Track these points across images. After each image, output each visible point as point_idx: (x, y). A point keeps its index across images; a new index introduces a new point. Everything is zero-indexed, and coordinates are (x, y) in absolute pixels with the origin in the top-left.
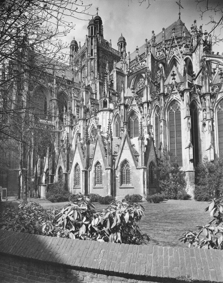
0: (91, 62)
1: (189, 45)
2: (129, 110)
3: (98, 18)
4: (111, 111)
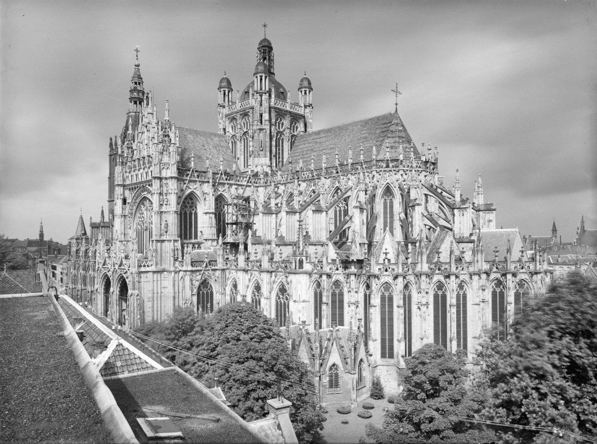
0: (259, 135)
1: (407, 170)
2: (332, 281)
3: (266, 44)
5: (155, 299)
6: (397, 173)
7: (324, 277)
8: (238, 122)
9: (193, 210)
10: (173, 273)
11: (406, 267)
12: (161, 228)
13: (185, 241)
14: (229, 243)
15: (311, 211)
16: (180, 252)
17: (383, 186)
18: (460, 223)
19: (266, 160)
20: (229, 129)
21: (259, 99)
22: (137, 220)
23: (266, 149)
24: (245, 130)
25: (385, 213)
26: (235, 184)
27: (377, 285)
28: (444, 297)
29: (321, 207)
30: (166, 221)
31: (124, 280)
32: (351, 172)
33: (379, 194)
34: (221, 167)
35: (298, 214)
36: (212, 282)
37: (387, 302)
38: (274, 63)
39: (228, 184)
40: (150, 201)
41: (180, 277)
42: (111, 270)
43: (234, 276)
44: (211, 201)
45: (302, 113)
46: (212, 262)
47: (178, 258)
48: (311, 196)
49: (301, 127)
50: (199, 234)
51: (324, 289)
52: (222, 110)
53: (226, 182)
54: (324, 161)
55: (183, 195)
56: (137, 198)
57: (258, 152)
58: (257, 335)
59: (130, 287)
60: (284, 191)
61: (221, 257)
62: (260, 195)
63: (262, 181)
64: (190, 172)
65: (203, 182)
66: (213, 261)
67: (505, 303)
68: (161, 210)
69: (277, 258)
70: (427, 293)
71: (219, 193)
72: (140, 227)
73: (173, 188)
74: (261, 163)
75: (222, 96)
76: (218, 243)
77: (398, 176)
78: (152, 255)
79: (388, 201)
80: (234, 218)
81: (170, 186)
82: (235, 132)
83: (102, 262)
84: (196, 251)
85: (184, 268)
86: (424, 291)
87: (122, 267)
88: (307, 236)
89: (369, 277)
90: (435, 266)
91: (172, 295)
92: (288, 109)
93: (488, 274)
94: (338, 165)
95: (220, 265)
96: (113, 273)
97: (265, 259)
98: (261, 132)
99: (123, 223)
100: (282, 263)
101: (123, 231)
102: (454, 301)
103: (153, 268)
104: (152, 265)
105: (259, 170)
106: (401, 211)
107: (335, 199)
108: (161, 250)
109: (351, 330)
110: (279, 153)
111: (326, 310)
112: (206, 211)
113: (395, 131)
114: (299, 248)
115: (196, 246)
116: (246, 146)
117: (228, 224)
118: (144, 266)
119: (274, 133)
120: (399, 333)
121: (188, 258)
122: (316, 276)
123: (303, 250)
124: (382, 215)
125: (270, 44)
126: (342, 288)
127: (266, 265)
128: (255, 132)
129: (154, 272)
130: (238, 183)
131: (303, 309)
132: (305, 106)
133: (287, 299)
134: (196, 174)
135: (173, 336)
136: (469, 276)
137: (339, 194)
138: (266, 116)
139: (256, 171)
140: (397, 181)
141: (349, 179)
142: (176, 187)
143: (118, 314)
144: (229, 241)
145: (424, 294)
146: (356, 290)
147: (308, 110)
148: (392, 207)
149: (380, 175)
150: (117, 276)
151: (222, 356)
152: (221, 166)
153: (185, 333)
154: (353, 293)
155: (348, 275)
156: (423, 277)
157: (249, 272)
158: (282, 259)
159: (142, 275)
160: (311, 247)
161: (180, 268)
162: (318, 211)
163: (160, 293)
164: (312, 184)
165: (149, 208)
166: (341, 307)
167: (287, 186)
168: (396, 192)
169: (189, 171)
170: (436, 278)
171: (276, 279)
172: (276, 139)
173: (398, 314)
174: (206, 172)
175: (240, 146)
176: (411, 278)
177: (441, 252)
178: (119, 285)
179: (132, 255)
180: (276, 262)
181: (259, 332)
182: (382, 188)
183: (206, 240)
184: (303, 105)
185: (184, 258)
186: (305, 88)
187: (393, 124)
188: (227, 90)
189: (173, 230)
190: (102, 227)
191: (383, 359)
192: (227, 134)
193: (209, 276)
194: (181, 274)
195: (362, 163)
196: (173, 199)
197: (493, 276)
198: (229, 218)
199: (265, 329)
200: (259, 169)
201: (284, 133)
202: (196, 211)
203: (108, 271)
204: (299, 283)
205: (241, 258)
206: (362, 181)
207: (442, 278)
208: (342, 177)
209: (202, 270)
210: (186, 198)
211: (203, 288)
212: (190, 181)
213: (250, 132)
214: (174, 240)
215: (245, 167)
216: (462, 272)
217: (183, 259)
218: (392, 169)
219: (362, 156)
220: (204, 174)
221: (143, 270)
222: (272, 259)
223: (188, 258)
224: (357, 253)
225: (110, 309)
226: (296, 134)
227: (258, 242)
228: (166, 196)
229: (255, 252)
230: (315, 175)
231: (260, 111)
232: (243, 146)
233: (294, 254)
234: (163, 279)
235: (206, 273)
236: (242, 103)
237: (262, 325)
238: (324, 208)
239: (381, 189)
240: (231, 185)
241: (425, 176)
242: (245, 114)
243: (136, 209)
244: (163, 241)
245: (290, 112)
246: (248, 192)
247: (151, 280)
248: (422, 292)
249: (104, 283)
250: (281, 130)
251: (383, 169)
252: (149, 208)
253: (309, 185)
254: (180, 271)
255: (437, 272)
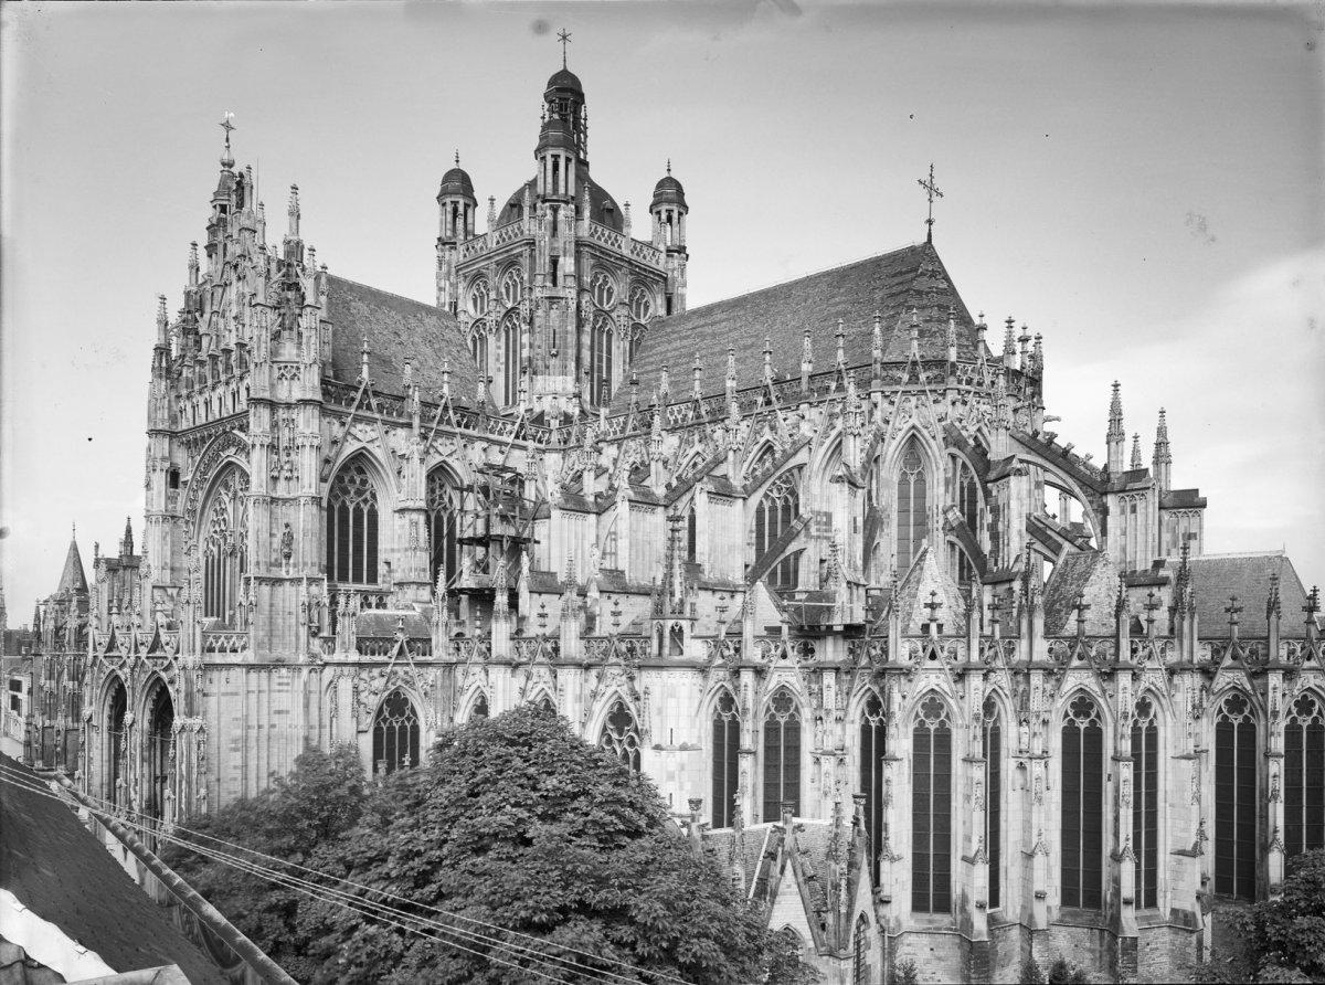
0: (547, 314)
1: (969, 392)
2: (771, 686)
4: (692, 666)
5: (252, 743)
6: (940, 398)
7: (747, 677)
8: (491, 284)
9: (365, 501)
10: (305, 671)
11: (990, 648)
12: (271, 543)
13: (342, 586)
14: (462, 591)
15: (705, 496)
16: (326, 612)
17: (901, 434)
18: (1124, 533)
19: (565, 382)
20: (466, 305)
21: (549, 217)
22: (207, 529)
23: (566, 353)
24: (509, 305)
25: (903, 511)
26: (480, 439)
27: (904, 697)
28: (1095, 735)
29: (730, 486)
30: (287, 526)
31: (164, 690)
32: (807, 398)
33: (888, 459)
34: (446, 389)
35: (660, 510)
36: (415, 698)
37: (933, 749)
38: (586, 137)
39: (463, 436)
40: (245, 475)
41: (326, 682)
42: (128, 661)
43: (478, 683)
44: (417, 474)
45: (660, 267)
46: (419, 643)
47: (319, 629)
48: (695, 465)
49: (658, 307)
50: (382, 569)
51: (745, 710)
52: (447, 253)
53: (458, 430)
54: (732, 372)
55: (338, 454)
56: (208, 466)
57: (544, 359)
58: (594, 822)
59: (179, 705)
60: (615, 461)
61: (441, 629)
62: (548, 474)
63: (555, 437)
64: (358, 396)
65: (396, 425)
66: (419, 640)
67: (1259, 756)
68: (274, 495)
69: (604, 627)
70: (1045, 723)
71: (439, 459)
72: (215, 550)
73: (307, 432)
74: (555, 391)
75: (450, 217)
76: (433, 593)
77: (944, 407)
78: (246, 621)
79: (912, 479)
80: (480, 523)
81: (301, 427)
82: (482, 309)
83: (106, 640)
84: (373, 611)
85: (338, 656)
86: (1038, 717)
87: (158, 654)
88: (692, 567)
89: (881, 674)
90: (1070, 647)
91: (301, 733)
92: (626, 252)
93: (1208, 672)
94: (770, 382)
95: (441, 649)
96: (133, 670)
97: (573, 628)
98: (555, 306)
99: (168, 538)
100: (621, 640)
101: (168, 561)
102: (1126, 746)
103: (250, 656)
104: (244, 648)
105: (547, 409)
106: (949, 503)
107: (768, 469)
108: (271, 605)
109: (837, 826)
110: (600, 368)
111: (751, 771)
112: (403, 505)
113: (927, 293)
114: (672, 594)
115: (373, 600)
116: (511, 349)
117: (461, 541)
118: (222, 650)
119: (588, 311)
120: (968, 839)
121: (347, 630)
122: (721, 674)
123: (682, 602)
124: (894, 516)
125: (580, 85)
126: (797, 709)
127: (572, 646)
128: (537, 306)
129: (250, 667)
130: (495, 437)
131: (683, 769)
132: (668, 251)
133: (632, 743)
134: (374, 402)
135: (291, 840)
136: (1166, 677)
137: (777, 456)
138: (567, 264)
139: (537, 410)
140: (940, 420)
141: (803, 417)
142: (316, 430)
143: (146, 786)
144: (464, 586)
145: (1038, 728)
146: (840, 714)
147: (676, 261)
148: (921, 495)
149: (892, 403)
150: (144, 678)
151: (457, 901)
152: (446, 387)
153: (327, 831)
154: (829, 724)
155: (818, 671)
156: (1037, 679)
157: (521, 669)
158: (621, 629)
159: (215, 675)
160: (702, 594)
161: (326, 658)
162: (724, 493)
163: (266, 726)
164: (697, 438)
165: (240, 494)
166: (794, 767)
167: (624, 447)
168: (937, 454)
169: (356, 389)
170: (1072, 682)
171: (602, 687)
172: (593, 329)
173: (966, 779)
174: (403, 399)
175: (495, 347)
176: (1003, 679)
177: (1087, 607)
178: (150, 705)
179: (186, 615)
180: (602, 639)
181: (597, 814)
182: (898, 439)
183: (400, 584)
184: (662, 248)
185: (338, 628)
186: (670, 202)
187: (922, 274)
188: (462, 202)
189: (307, 547)
190: (125, 568)
191: (925, 916)
192: (462, 317)
193: (407, 682)
194: (329, 673)
195: (840, 372)
196: (308, 463)
197: (1223, 680)
198: (469, 526)
199: (620, 801)
200: (546, 405)
201: (614, 315)
202: (372, 505)
203: (121, 667)
204: (672, 695)
205: (501, 630)
206: (853, 409)
207: (1090, 682)
208: (781, 415)
209: (387, 664)
210: (345, 468)
211: (392, 715)
212: (357, 419)
213: (524, 309)
214: (308, 579)
215: (507, 402)
216: (1148, 664)
217: (334, 633)
218: (927, 388)
219: (841, 352)
220: (398, 405)
221: (218, 662)
222: (590, 629)
223: (347, 630)
224: (849, 609)
225: (121, 773)
226: (643, 322)
227: (546, 585)
228: (288, 455)
229: (541, 611)
230: (704, 413)
231: (552, 249)
232: (503, 347)
233: (658, 612)
234: (278, 688)
235: (401, 673)
236: (504, 231)
237: (606, 787)
238: (739, 489)
239: (895, 443)
240: (471, 439)
241: (1015, 411)
242: (510, 264)
243: (206, 499)
244: (279, 581)
245: (630, 262)
246: (519, 461)
247: (242, 691)
248: (1033, 720)
249: (109, 701)
250: (606, 308)
251: (901, 388)
252: (240, 494)
253: (687, 442)
254: (326, 664)
255: (1075, 662)
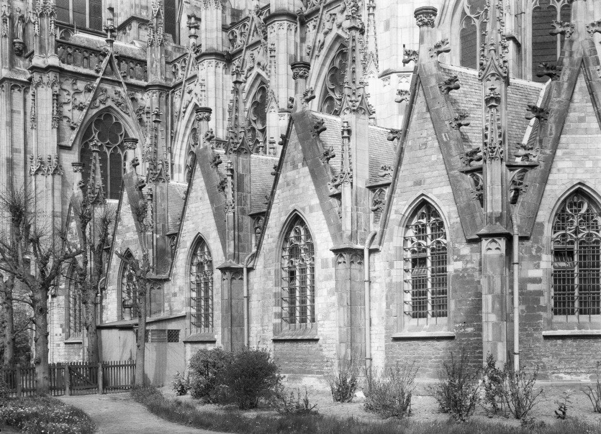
193: (119, 104)
